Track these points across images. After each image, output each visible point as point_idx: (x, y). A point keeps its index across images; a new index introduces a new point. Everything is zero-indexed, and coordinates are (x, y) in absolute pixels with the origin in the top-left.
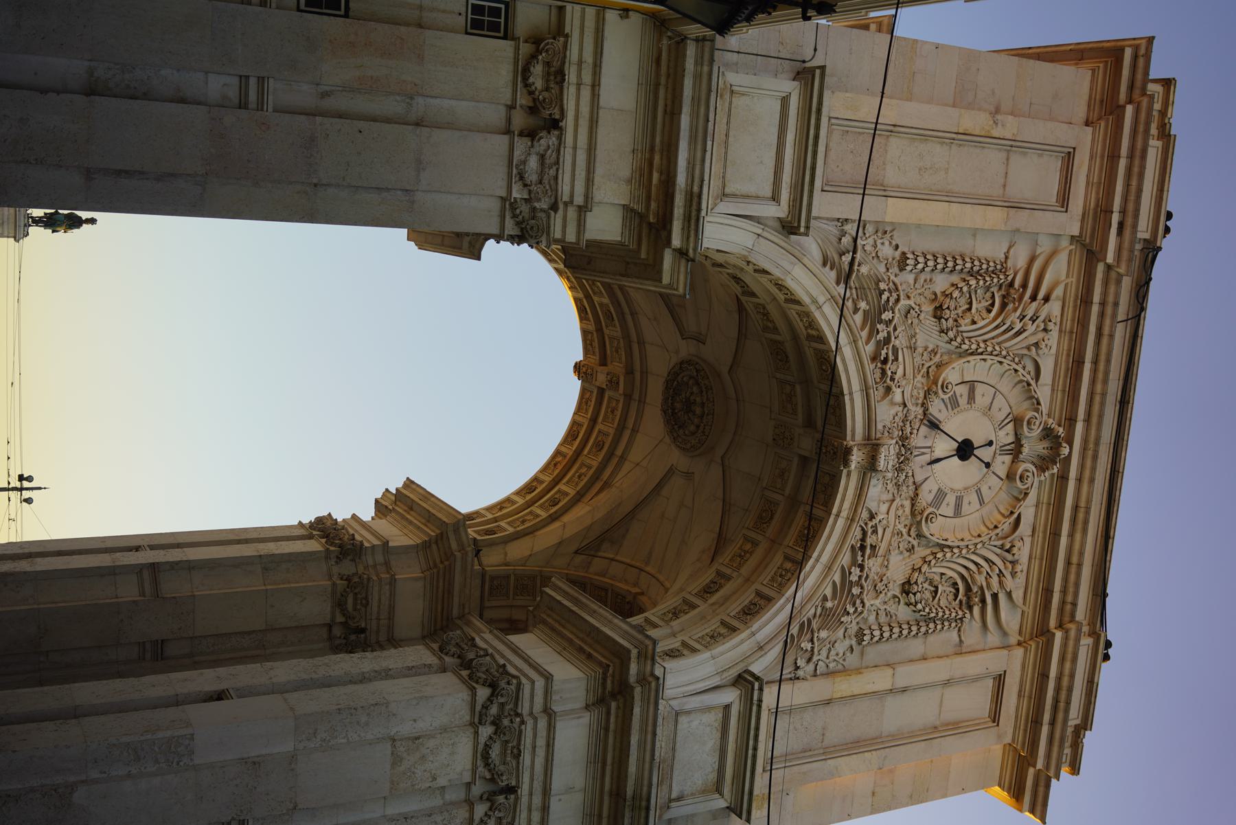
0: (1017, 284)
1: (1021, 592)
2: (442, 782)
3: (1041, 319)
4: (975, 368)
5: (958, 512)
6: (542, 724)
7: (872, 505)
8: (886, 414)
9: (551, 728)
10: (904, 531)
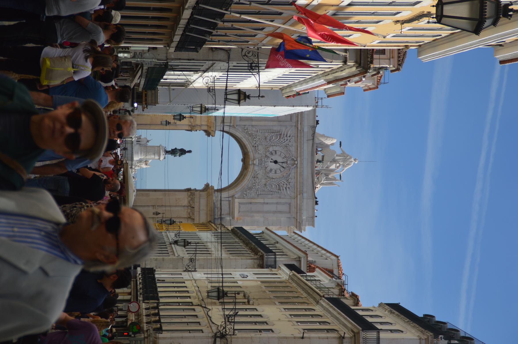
0: (282, 134)
1: (293, 189)
2: (183, 205)
3: (289, 140)
4: (275, 148)
5: (276, 173)
7: (257, 171)
8: (257, 156)
10: (264, 175)
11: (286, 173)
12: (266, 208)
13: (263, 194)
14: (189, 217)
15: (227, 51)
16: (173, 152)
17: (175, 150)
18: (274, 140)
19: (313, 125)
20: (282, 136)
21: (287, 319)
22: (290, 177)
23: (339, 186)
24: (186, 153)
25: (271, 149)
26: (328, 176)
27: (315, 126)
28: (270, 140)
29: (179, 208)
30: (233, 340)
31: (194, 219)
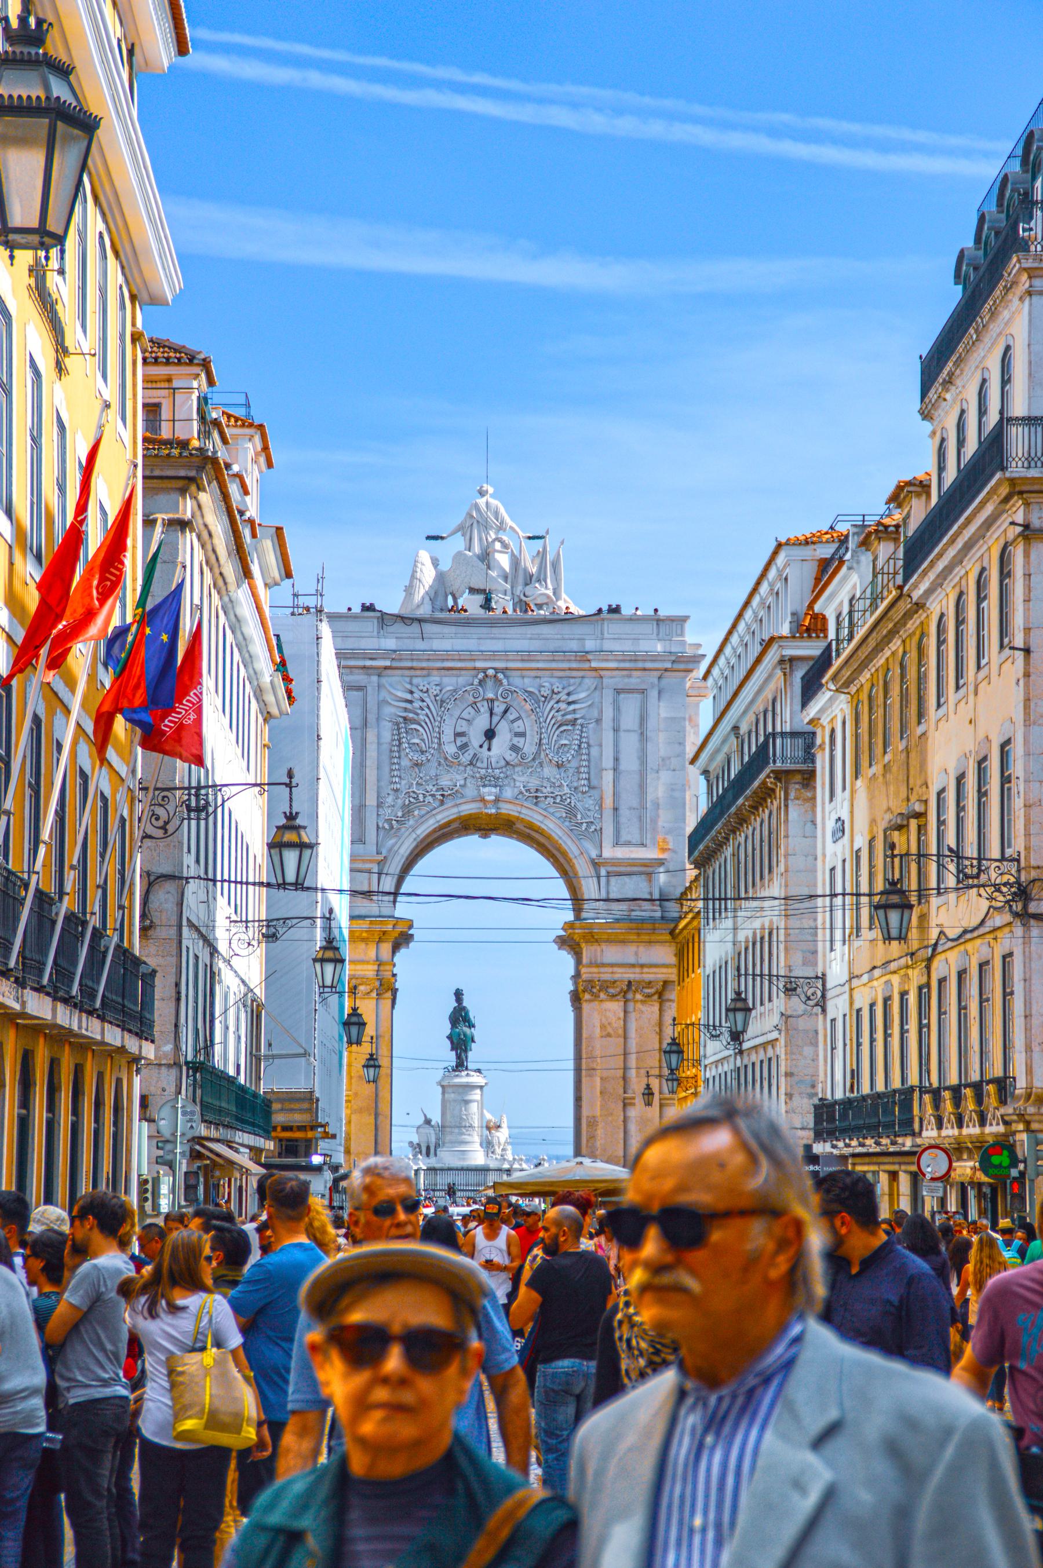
0: (404, 714)
1: (572, 681)
2: (622, 1015)
3: (421, 694)
4: (448, 736)
5: (522, 735)
6: (602, 970)
7: (516, 791)
8: (470, 791)
9: (603, 965)
11: (523, 703)
12: (630, 763)
13: (589, 773)
14: (660, 997)
15: (150, 884)
16: (460, 1045)
17: (455, 1041)
18: (423, 740)
19: (376, 621)
20: (411, 715)
21: (971, 697)
22: (537, 692)
23: (562, 543)
24: (464, 1008)
25: (450, 749)
26: (531, 576)
27: (379, 614)
28: (422, 752)
29: (633, 1026)
30: (1033, 863)
31: (666, 983)
